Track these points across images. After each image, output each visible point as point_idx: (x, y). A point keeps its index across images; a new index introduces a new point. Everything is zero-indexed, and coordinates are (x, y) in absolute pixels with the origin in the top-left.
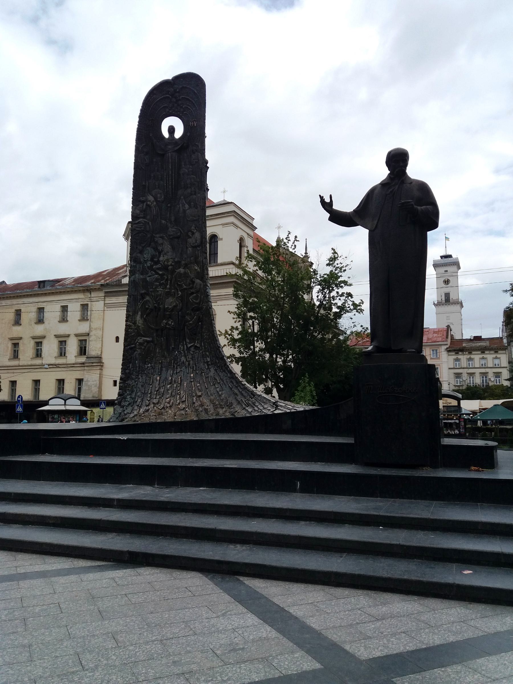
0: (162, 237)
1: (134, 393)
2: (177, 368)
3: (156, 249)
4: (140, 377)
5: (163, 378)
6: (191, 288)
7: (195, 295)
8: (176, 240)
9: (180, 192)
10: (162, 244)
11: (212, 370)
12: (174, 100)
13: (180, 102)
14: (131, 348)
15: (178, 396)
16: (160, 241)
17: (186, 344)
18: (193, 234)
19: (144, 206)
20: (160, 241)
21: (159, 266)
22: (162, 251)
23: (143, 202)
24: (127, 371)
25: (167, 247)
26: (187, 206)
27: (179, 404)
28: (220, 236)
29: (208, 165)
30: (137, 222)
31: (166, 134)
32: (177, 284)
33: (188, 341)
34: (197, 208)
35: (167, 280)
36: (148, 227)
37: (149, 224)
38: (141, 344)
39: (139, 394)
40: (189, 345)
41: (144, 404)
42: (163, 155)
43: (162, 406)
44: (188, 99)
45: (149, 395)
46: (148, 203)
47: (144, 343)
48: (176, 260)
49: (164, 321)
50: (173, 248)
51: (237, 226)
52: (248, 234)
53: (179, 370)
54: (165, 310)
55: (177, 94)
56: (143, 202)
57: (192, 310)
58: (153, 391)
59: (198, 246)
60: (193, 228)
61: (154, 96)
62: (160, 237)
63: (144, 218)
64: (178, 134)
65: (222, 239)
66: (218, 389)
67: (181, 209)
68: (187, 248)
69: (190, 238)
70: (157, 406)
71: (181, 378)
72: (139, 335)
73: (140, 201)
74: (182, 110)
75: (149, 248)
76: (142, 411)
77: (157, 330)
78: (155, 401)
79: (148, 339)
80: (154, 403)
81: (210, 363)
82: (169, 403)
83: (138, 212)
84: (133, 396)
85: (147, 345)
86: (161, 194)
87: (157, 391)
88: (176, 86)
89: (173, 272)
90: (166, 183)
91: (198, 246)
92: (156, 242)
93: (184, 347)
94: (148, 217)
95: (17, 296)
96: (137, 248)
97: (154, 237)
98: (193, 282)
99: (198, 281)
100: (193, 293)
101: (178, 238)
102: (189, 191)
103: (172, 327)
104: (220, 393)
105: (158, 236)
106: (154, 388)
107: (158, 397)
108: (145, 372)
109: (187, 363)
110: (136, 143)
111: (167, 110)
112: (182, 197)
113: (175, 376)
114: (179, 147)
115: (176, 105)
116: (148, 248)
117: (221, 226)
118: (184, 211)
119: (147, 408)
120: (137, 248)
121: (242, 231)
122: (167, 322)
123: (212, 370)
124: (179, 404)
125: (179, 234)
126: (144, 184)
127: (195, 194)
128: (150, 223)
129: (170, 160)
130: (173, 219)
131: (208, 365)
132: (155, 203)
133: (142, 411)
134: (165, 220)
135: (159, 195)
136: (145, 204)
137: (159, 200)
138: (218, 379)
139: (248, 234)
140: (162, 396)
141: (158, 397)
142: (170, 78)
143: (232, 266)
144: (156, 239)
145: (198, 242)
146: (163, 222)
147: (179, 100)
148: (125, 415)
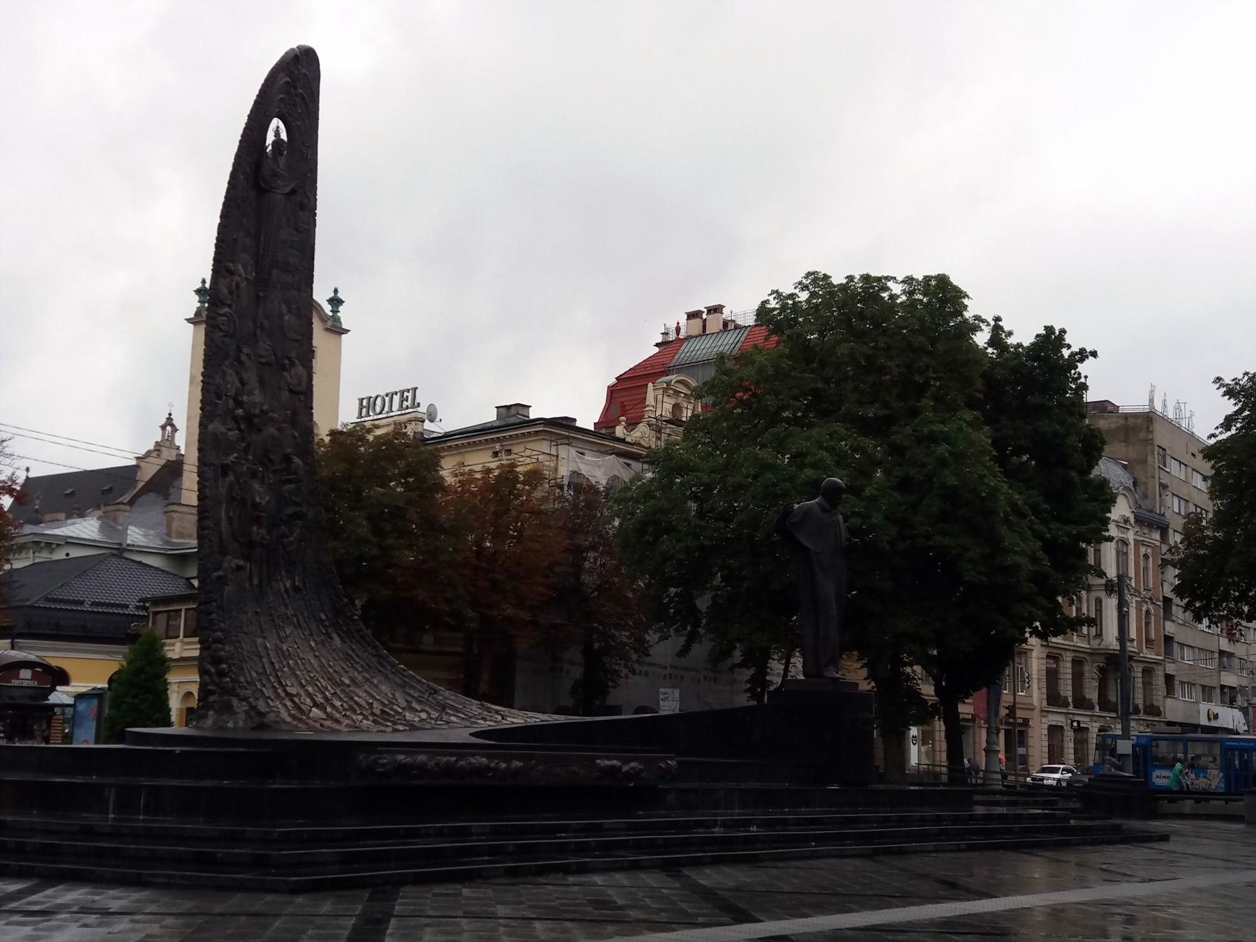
7: (292, 486)
14: (219, 578)
16: (247, 363)
18: (292, 364)
25: (252, 377)
35: (249, 445)
48: (265, 407)
50: (262, 382)
54: (256, 506)
63: (230, 306)
92: (241, 362)
99: (296, 460)
100: (289, 481)
101: (269, 364)
118: (281, 315)
144: (244, 358)
145: (304, 384)
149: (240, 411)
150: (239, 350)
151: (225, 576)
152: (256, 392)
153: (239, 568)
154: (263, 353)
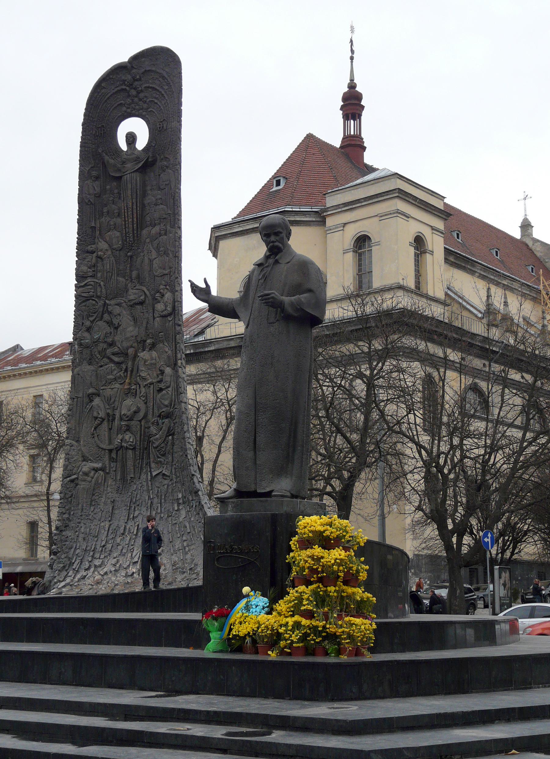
0: (119, 304)
1: (73, 550)
2: (134, 510)
3: (110, 323)
4: (82, 524)
5: (113, 527)
6: (160, 381)
8: (138, 307)
9: (145, 232)
10: (119, 315)
11: (183, 513)
12: (133, 92)
13: (141, 95)
14: (72, 481)
15: (130, 555)
16: (117, 310)
17: (150, 471)
19: (94, 259)
20: (117, 310)
21: (116, 350)
22: (119, 325)
23: (92, 252)
24: (66, 516)
25: (125, 319)
26: (154, 254)
27: (129, 566)
28: (375, 239)
29: (363, 103)
30: (82, 284)
31: (123, 145)
32: (140, 376)
33: (153, 465)
34: (168, 255)
35: (126, 370)
36: (99, 289)
37: (100, 285)
38: (86, 474)
39: (78, 551)
40: (154, 474)
41: (83, 567)
42: (120, 178)
43: (105, 570)
44: (153, 88)
45: (91, 553)
46: (100, 253)
47: (90, 472)
49: (120, 437)
50: (135, 320)
51: (407, 216)
52: (433, 228)
53: (136, 513)
55: (136, 83)
56: (92, 252)
57: (159, 416)
58: (98, 547)
59: (170, 315)
60: (162, 287)
61: (103, 91)
62: (116, 305)
63: (91, 276)
64: (141, 143)
65: (378, 244)
66: (185, 544)
67: (146, 261)
68: (154, 318)
69: (159, 302)
70: (99, 569)
71: (138, 525)
72: (85, 459)
73: (88, 252)
74: (145, 106)
75: (100, 323)
76: (79, 576)
77: (110, 451)
78: (97, 562)
79: (96, 465)
80: (96, 566)
81: (181, 501)
82: (114, 565)
83: (85, 268)
84: (70, 556)
85: (95, 474)
86: (118, 237)
87: (104, 546)
88: (134, 71)
89: (135, 356)
90: (125, 221)
91: (170, 315)
92: (110, 313)
93: (147, 476)
94: (99, 275)
95: (36, 372)
96: (83, 323)
97: (108, 305)
98: (162, 372)
100: (161, 390)
101: (142, 303)
102: (156, 229)
103: (131, 445)
104: (187, 549)
105: (113, 302)
106: (99, 543)
107: (102, 556)
108: (90, 517)
109: (150, 501)
110: (80, 164)
111: (124, 109)
112: (148, 240)
113: (130, 523)
114: (140, 165)
115: (136, 99)
116: (98, 323)
117: (377, 219)
118: (151, 261)
119: (85, 574)
120: (83, 323)
121: (421, 223)
122: (123, 437)
123: (183, 513)
124: (129, 566)
125: (142, 298)
126: (93, 225)
127: (165, 234)
128: (102, 283)
129: (129, 186)
130: (134, 274)
131: (179, 504)
132: (109, 252)
133: (79, 576)
134: (124, 277)
135: (114, 241)
136: (95, 255)
137: (115, 247)
138: (188, 527)
139: (433, 228)
140: (110, 554)
141: (102, 556)
142: (126, 59)
143: (400, 293)
144: (110, 308)
145: (169, 309)
146: (121, 279)
147: (142, 91)
148: (56, 583)
149: (109, 351)
150: (105, 304)
151: (77, 478)
152: (131, 328)
153: (96, 470)
154: (132, 297)
